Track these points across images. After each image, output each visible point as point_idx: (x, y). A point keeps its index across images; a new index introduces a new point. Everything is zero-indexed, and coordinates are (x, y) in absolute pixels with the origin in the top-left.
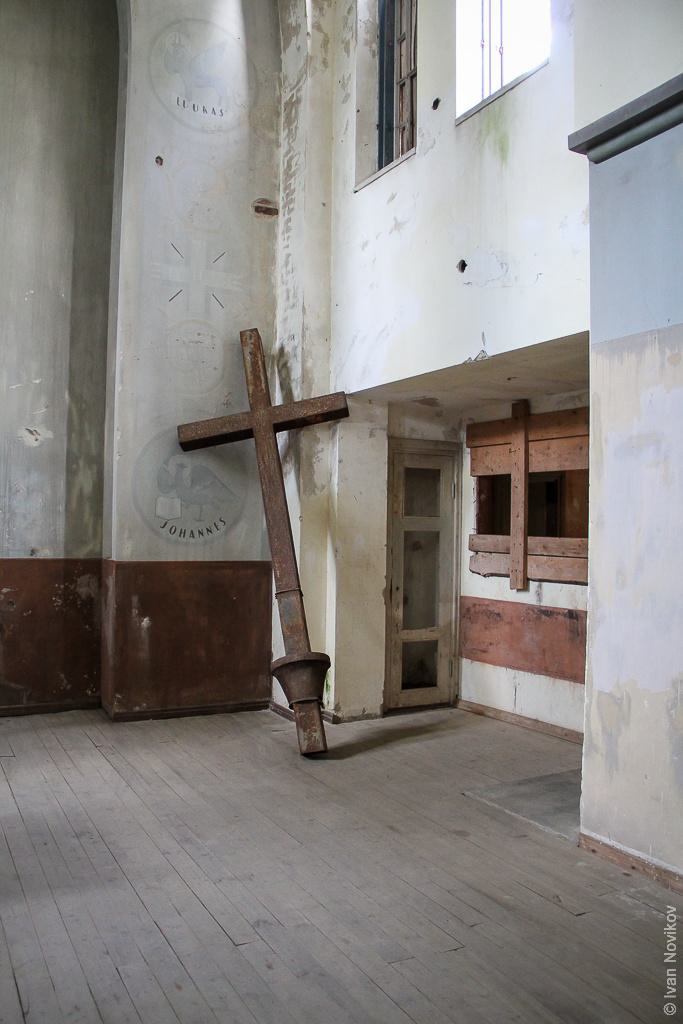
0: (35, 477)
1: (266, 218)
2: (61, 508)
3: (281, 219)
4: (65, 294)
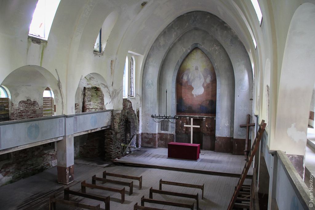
0: (227, 129)
1: (252, 101)
3: (253, 101)
4: (230, 109)
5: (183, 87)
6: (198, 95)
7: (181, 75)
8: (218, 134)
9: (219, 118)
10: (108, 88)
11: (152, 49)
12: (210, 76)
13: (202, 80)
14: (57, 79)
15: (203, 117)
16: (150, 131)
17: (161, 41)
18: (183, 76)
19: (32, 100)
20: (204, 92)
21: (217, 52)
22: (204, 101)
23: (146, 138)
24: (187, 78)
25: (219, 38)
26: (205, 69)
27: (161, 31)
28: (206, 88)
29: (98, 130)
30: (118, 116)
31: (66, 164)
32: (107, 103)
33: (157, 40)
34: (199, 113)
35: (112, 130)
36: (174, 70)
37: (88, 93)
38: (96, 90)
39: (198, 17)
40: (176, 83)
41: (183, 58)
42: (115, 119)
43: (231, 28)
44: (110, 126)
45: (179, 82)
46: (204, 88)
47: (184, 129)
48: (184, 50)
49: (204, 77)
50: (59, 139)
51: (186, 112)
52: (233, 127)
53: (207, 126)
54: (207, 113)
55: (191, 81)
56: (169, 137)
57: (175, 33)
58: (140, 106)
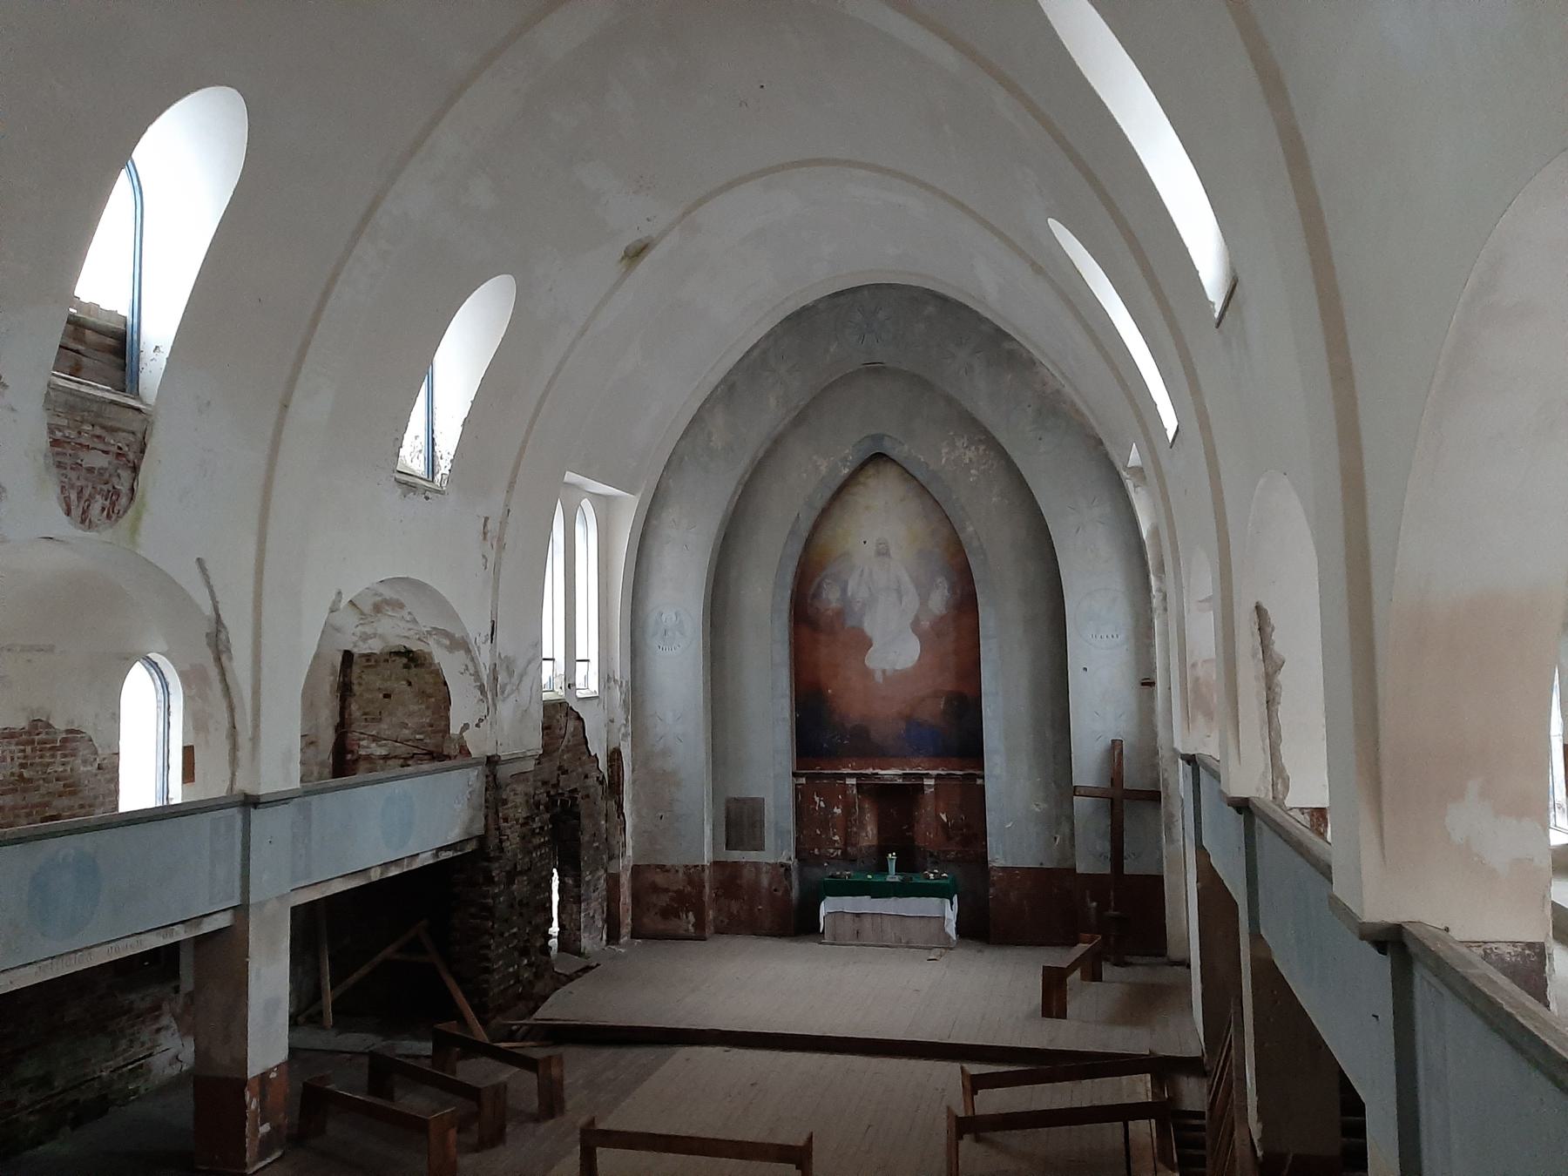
8: (998, 856)
10: (468, 651)
11: (673, 464)
13: (911, 600)
14: (208, 610)
15: (921, 776)
16: (676, 857)
18: (819, 586)
19: (60, 724)
23: (655, 889)
27: (715, 378)
29: (417, 864)
30: (520, 788)
31: (243, 1064)
32: (466, 726)
33: (696, 420)
35: (489, 860)
37: (367, 684)
38: (406, 666)
39: (881, 315)
41: (820, 504)
42: (505, 802)
44: (482, 839)
46: (920, 637)
48: (823, 469)
50: (208, 927)
52: (1070, 819)
53: (944, 817)
56: (765, 881)
58: (625, 735)
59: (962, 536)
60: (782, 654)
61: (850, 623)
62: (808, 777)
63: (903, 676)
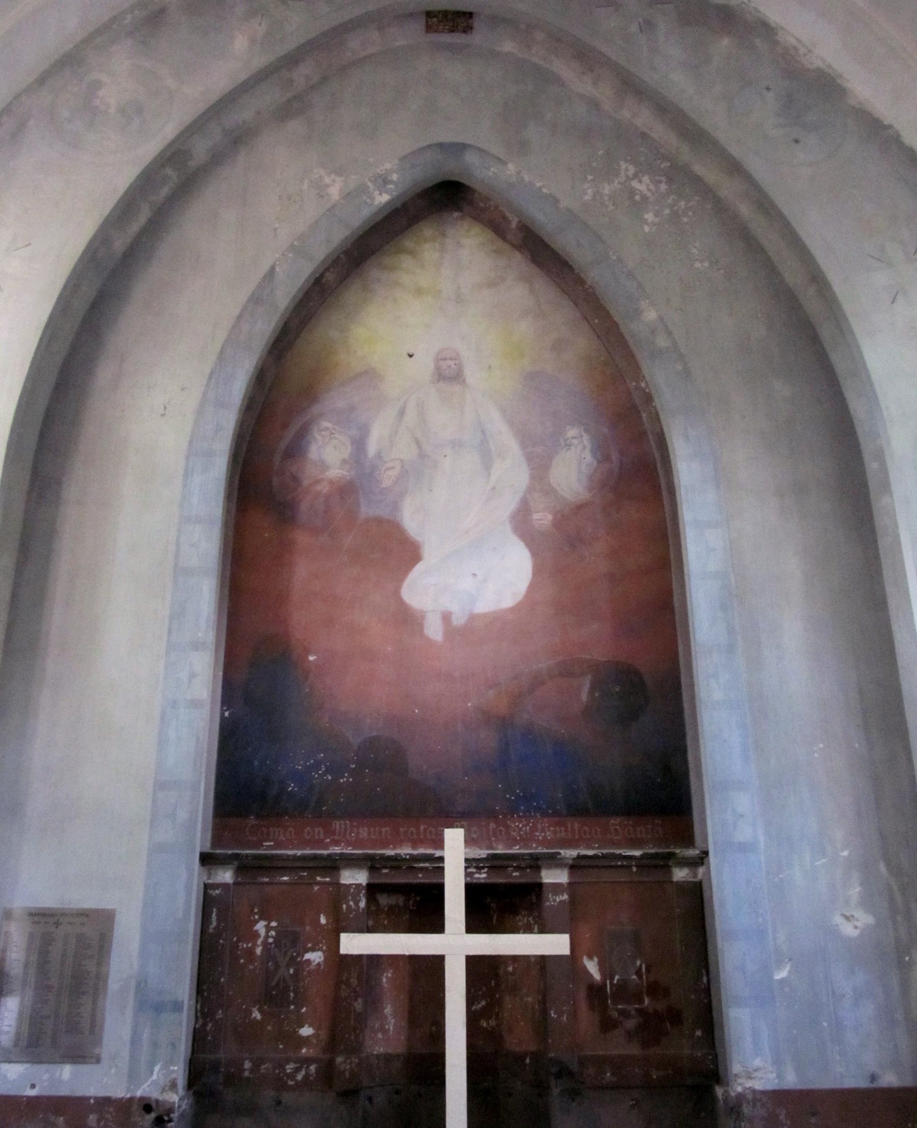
2: (899, 1016)
5: (302, 539)
6: (473, 617)
7: (285, 426)
9: (746, 848)
12: (586, 439)
13: (512, 473)
15: (536, 863)
17: (104, 78)
18: (303, 434)
20: (532, 587)
21: (650, 217)
22: (537, 682)
24: (346, 451)
25: (677, 81)
26: (532, 378)
28: (559, 544)
33: (70, 62)
34: (492, 815)
36: (212, 358)
40: (228, 497)
43: (774, 16)
45: (262, 487)
47: (306, 1031)
48: (335, 192)
49: (523, 445)
51: (332, 815)
54: (577, 810)
55: (387, 478)
57: (260, 27)
59: (634, 329)
60: (205, 545)
61: (366, 511)
62: (248, 868)
63: (496, 625)
